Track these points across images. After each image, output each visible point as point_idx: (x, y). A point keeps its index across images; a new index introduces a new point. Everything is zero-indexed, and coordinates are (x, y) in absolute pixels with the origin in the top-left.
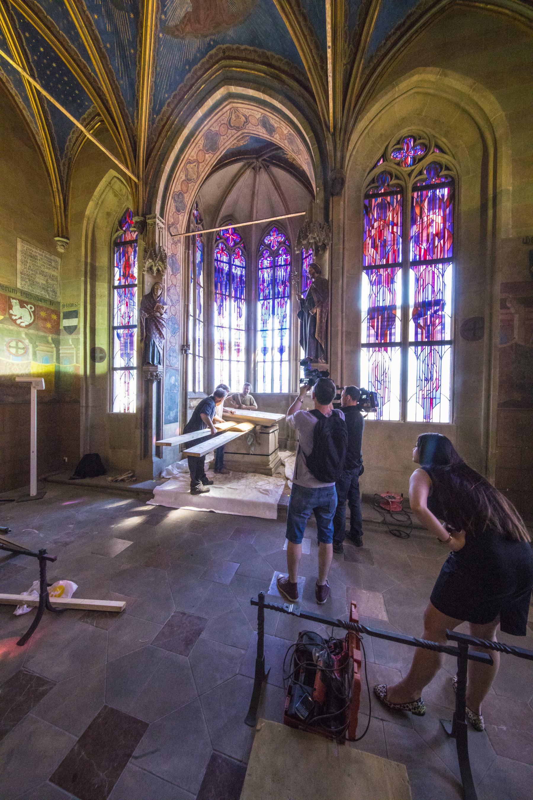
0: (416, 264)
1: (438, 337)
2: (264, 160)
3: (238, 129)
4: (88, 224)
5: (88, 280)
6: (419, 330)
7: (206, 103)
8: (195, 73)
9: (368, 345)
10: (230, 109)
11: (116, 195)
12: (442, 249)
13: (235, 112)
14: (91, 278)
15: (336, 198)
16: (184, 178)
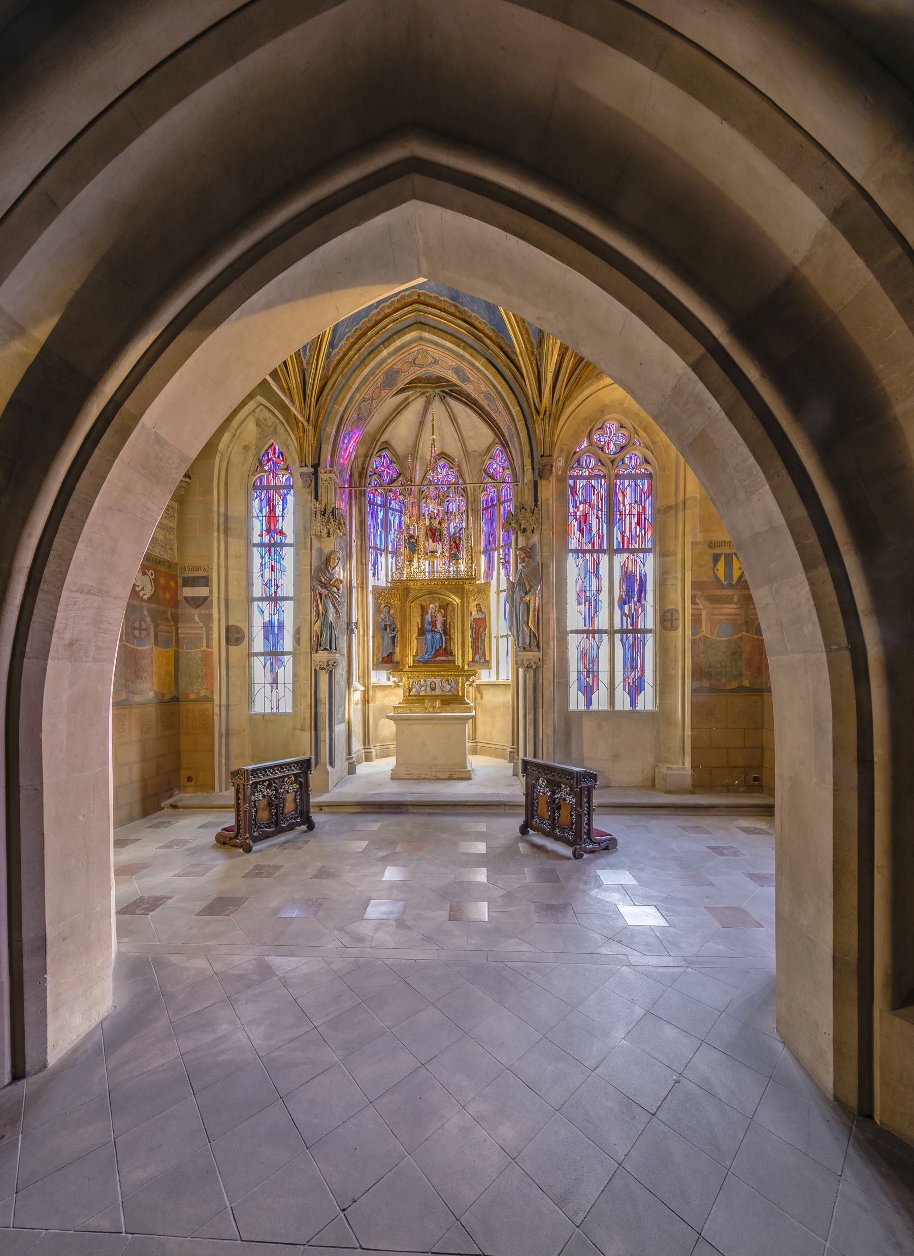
0: (619, 551)
1: (640, 626)
2: (443, 392)
3: (421, 366)
4: (221, 460)
5: (222, 536)
6: (625, 618)
8: (382, 309)
9: (578, 632)
11: (258, 425)
12: (644, 538)
14: (226, 535)
15: (544, 482)
16: (355, 417)
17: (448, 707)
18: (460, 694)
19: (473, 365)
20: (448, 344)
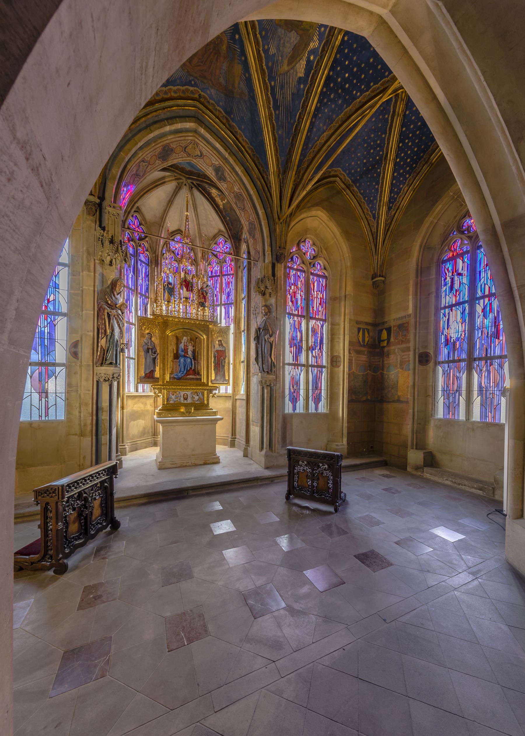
3: (189, 155)
7: (175, 125)
10: (192, 140)
13: (194, 144)
17: (200, 412)
18: (206, 402)
19: (233, 169)
20: (218, 145)
